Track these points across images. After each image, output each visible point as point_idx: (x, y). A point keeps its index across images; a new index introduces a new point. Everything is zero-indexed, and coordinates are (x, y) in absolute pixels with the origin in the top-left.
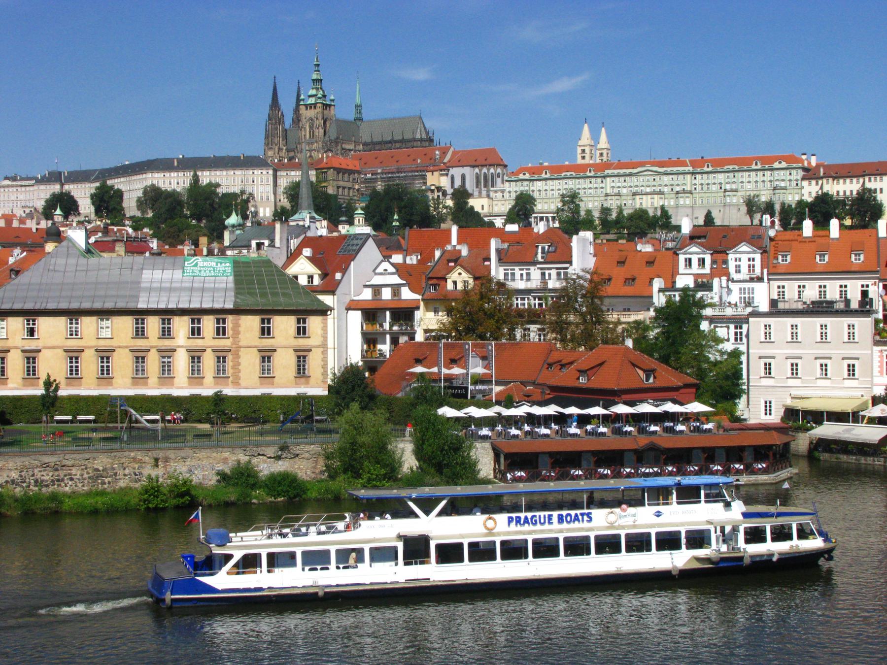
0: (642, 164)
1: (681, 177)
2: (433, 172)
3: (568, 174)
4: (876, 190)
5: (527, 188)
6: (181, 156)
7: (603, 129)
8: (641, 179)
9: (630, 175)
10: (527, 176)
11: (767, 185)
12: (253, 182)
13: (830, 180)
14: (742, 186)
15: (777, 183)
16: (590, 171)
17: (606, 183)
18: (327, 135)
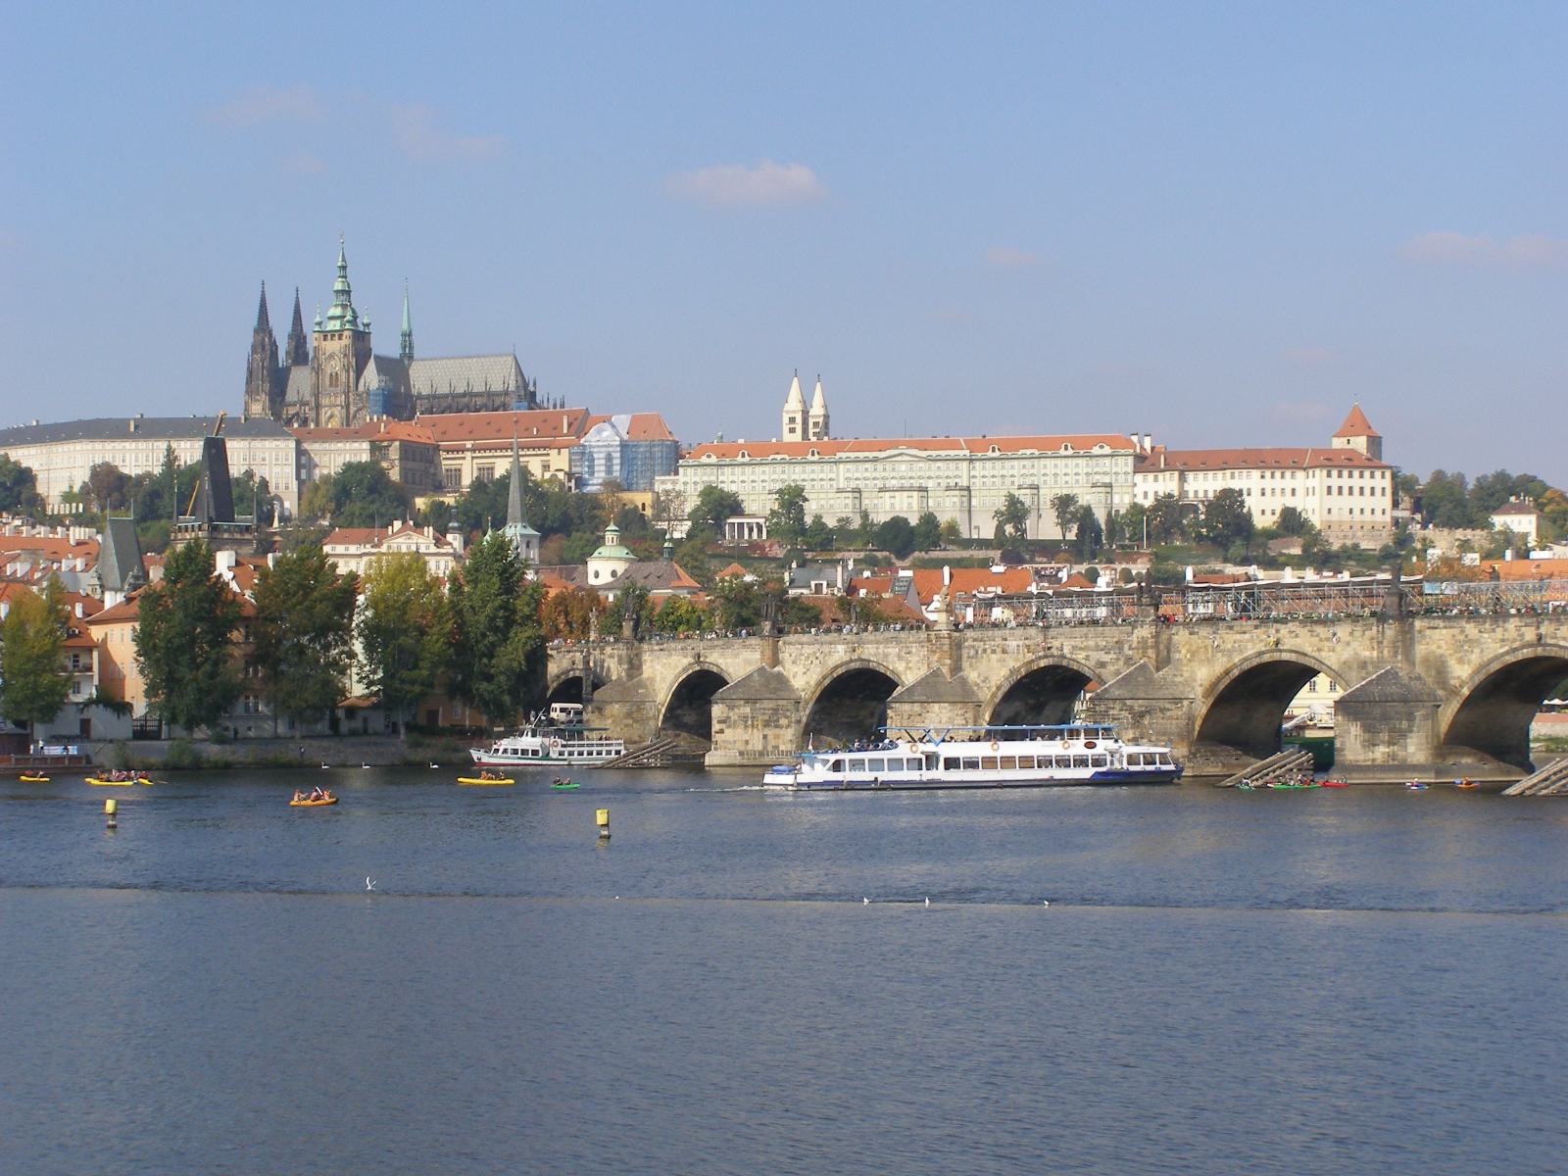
0: (894, 445)
1: (952, 465)
2: (559, 449)
3: (779, 457)
4: (1241, 491)
5: (713, 478)
6: (139, 416)
7: (818, 384)
8: (889, 466)
9: (876, 460)
10: (714, 459)
11: (1082, 478)
12: (264, 459)
13: (1176, 473)
14: (1045, 481)
15: (1097, 477)
16: (813, 454)
17: (838, 472)
18: (362, 381)
